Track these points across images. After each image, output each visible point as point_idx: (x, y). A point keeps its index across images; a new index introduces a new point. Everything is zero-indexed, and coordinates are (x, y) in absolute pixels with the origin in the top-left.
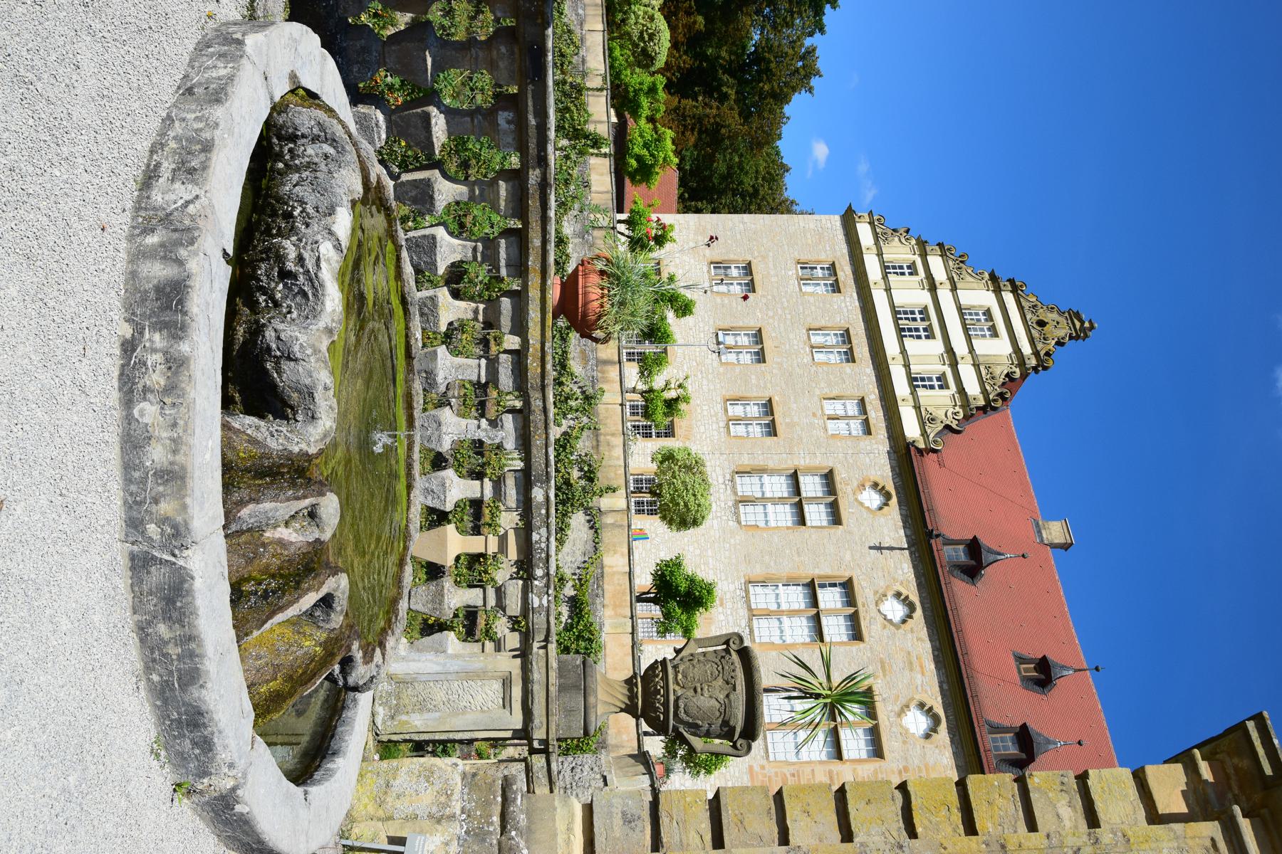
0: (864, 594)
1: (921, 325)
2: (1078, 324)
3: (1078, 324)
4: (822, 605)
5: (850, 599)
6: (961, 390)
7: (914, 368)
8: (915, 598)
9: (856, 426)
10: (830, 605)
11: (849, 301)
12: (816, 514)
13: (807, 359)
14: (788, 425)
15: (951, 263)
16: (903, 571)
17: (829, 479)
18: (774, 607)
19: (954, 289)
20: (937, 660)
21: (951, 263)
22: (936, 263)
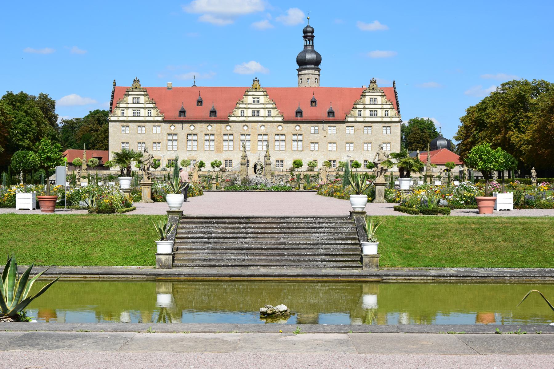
0: (190, 132)
1: (136, 112)
2: (136, 81)
3: (136, 81)
4: (191, 139)
5: (191, 134)
6: (152, 108)
7: (147, 115)
8: (191, 124)
9: (159, 128)
10: (191, 137)
11: (131, 124)
12: (175, 137)
13: (144, 134)
14: (158, 140)
15: (121, 102)
16: (186, 125)
17: (168, 134)
18: (191, 146)
19: (129, 104)
20: (201, 123)
21: (121, 102)
22: (121, 105)
